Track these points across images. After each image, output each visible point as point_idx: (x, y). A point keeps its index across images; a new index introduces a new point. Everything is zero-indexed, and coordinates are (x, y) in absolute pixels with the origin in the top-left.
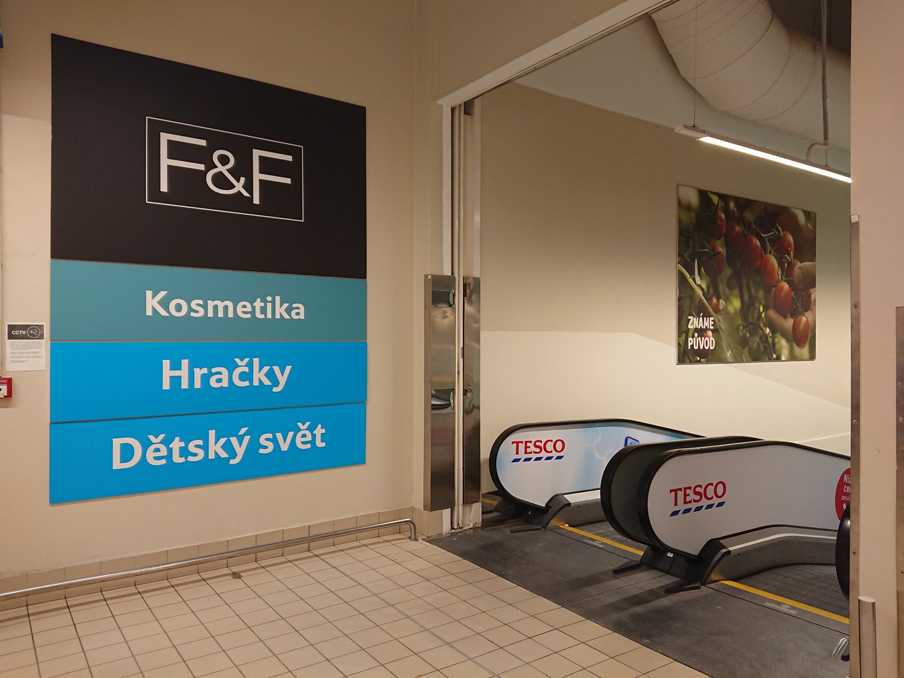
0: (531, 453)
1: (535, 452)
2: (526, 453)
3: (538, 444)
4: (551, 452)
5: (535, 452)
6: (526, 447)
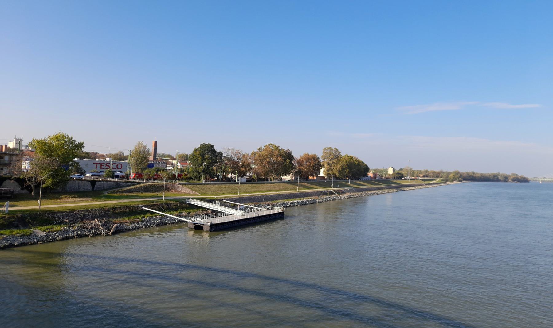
0: (104, 168)
1: (106, 168)
2: (101, 168)
3: (107, 164)
4: (115, 169)
5: (106, 168)
6: (101, 166)
